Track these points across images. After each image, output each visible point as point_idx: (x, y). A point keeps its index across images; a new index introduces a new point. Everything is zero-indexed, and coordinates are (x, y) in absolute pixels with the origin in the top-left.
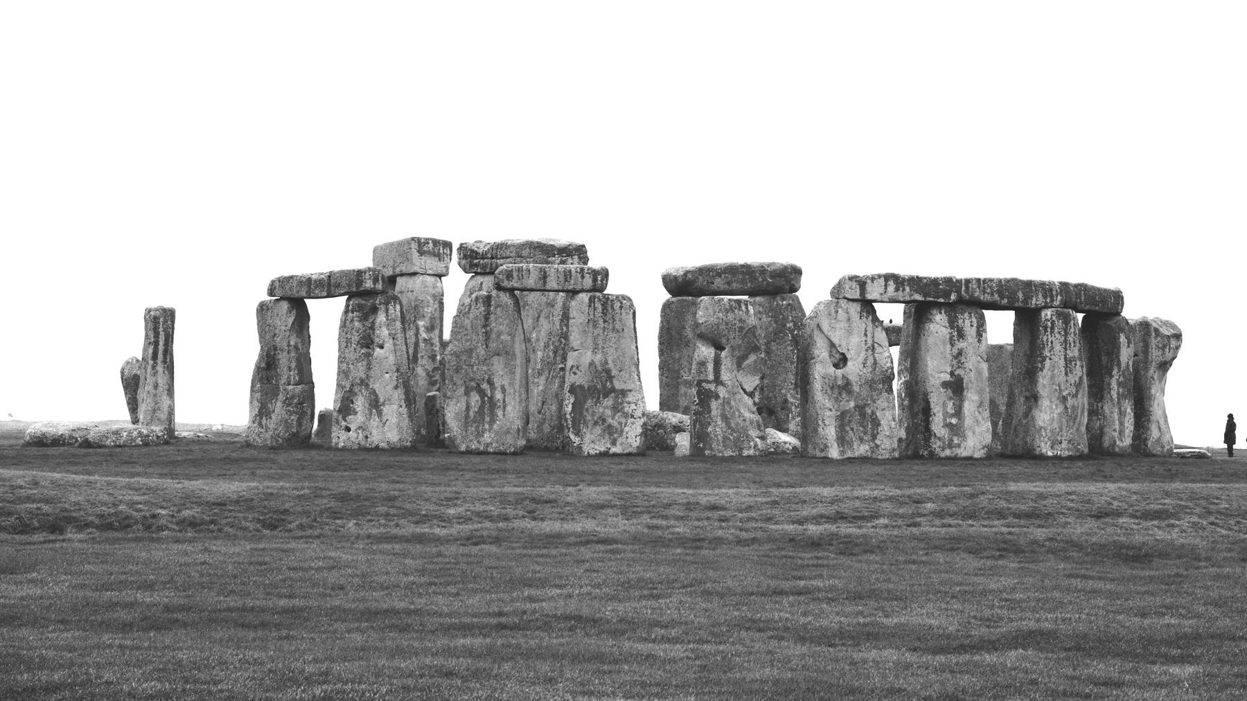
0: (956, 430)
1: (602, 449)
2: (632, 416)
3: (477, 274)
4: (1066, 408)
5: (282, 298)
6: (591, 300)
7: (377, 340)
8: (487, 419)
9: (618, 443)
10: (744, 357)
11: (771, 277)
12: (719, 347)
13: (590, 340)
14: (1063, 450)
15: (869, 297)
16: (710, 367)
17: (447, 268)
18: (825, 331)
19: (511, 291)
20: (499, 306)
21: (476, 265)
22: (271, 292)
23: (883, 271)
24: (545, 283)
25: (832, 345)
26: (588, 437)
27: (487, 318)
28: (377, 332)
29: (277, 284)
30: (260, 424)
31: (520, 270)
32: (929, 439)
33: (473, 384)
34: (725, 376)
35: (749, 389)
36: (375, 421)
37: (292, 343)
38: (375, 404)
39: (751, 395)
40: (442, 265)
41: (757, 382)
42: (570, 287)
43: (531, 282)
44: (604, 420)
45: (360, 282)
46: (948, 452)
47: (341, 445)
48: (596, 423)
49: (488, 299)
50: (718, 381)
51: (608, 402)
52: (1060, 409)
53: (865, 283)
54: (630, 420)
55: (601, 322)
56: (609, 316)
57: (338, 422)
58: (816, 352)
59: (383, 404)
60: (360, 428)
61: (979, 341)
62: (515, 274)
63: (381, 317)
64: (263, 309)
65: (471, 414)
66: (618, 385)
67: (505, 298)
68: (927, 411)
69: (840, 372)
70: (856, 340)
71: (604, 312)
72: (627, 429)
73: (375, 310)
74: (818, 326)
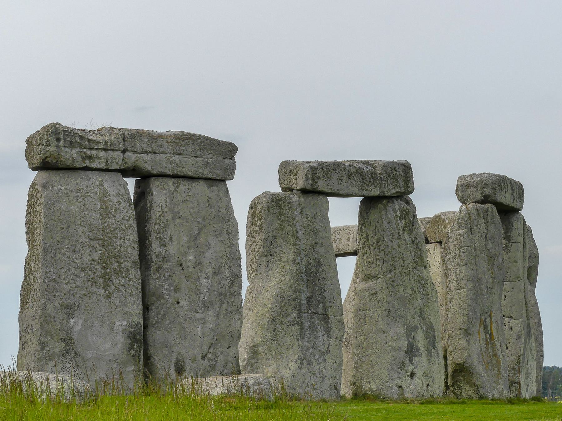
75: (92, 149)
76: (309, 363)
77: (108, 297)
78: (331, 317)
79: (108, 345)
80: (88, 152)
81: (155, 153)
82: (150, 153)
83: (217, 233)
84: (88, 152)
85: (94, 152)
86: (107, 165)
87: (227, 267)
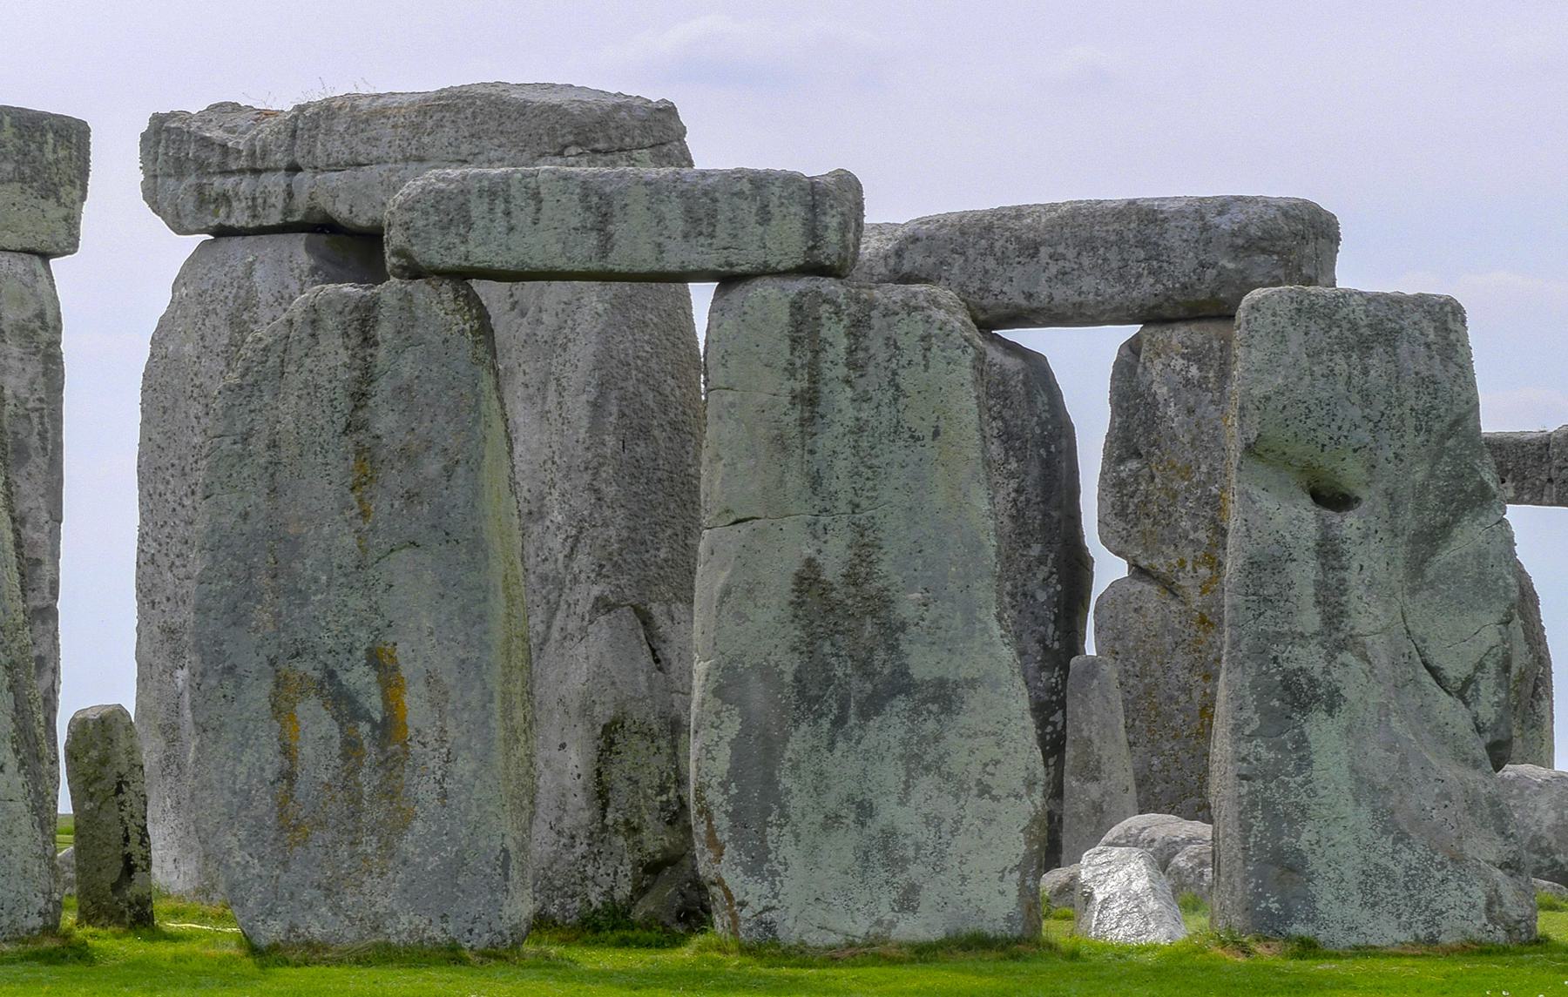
1: (860, 927)
2: (984, 790)
3: (222, 232)
6: (796, 307)
10: (1432, 538)
11: (1236, 251)
13: (795, 481)
16: (1304, 574)
17: (71, 224)
19: (461, 276)
21: (225, 199)
24: (606, 245)
26: (793, 888)
27: (360, 398)
31: (494, 192)
34: (1368, 617)
35: (1455, 670)
39: (1464, 691)
40: (53, 211)
41: (1491, 636)
43: (540, 248)
44: (865, 810)
48: (832, 821)
50: (1335, 630)
51: (889, 730)
54: (974, 806)
55: (844, 396)
62: (478, 209)
65: (301, 787)
66: (923, 664)
72: (961, 842)
75: (232, 173)
80: (218, 183)
81: (360, 165)
82: (347, 164)
83: (531, 390)
84: (218, 183)
85: (230, 181)
86: (254, 216)
87: (556, 494)
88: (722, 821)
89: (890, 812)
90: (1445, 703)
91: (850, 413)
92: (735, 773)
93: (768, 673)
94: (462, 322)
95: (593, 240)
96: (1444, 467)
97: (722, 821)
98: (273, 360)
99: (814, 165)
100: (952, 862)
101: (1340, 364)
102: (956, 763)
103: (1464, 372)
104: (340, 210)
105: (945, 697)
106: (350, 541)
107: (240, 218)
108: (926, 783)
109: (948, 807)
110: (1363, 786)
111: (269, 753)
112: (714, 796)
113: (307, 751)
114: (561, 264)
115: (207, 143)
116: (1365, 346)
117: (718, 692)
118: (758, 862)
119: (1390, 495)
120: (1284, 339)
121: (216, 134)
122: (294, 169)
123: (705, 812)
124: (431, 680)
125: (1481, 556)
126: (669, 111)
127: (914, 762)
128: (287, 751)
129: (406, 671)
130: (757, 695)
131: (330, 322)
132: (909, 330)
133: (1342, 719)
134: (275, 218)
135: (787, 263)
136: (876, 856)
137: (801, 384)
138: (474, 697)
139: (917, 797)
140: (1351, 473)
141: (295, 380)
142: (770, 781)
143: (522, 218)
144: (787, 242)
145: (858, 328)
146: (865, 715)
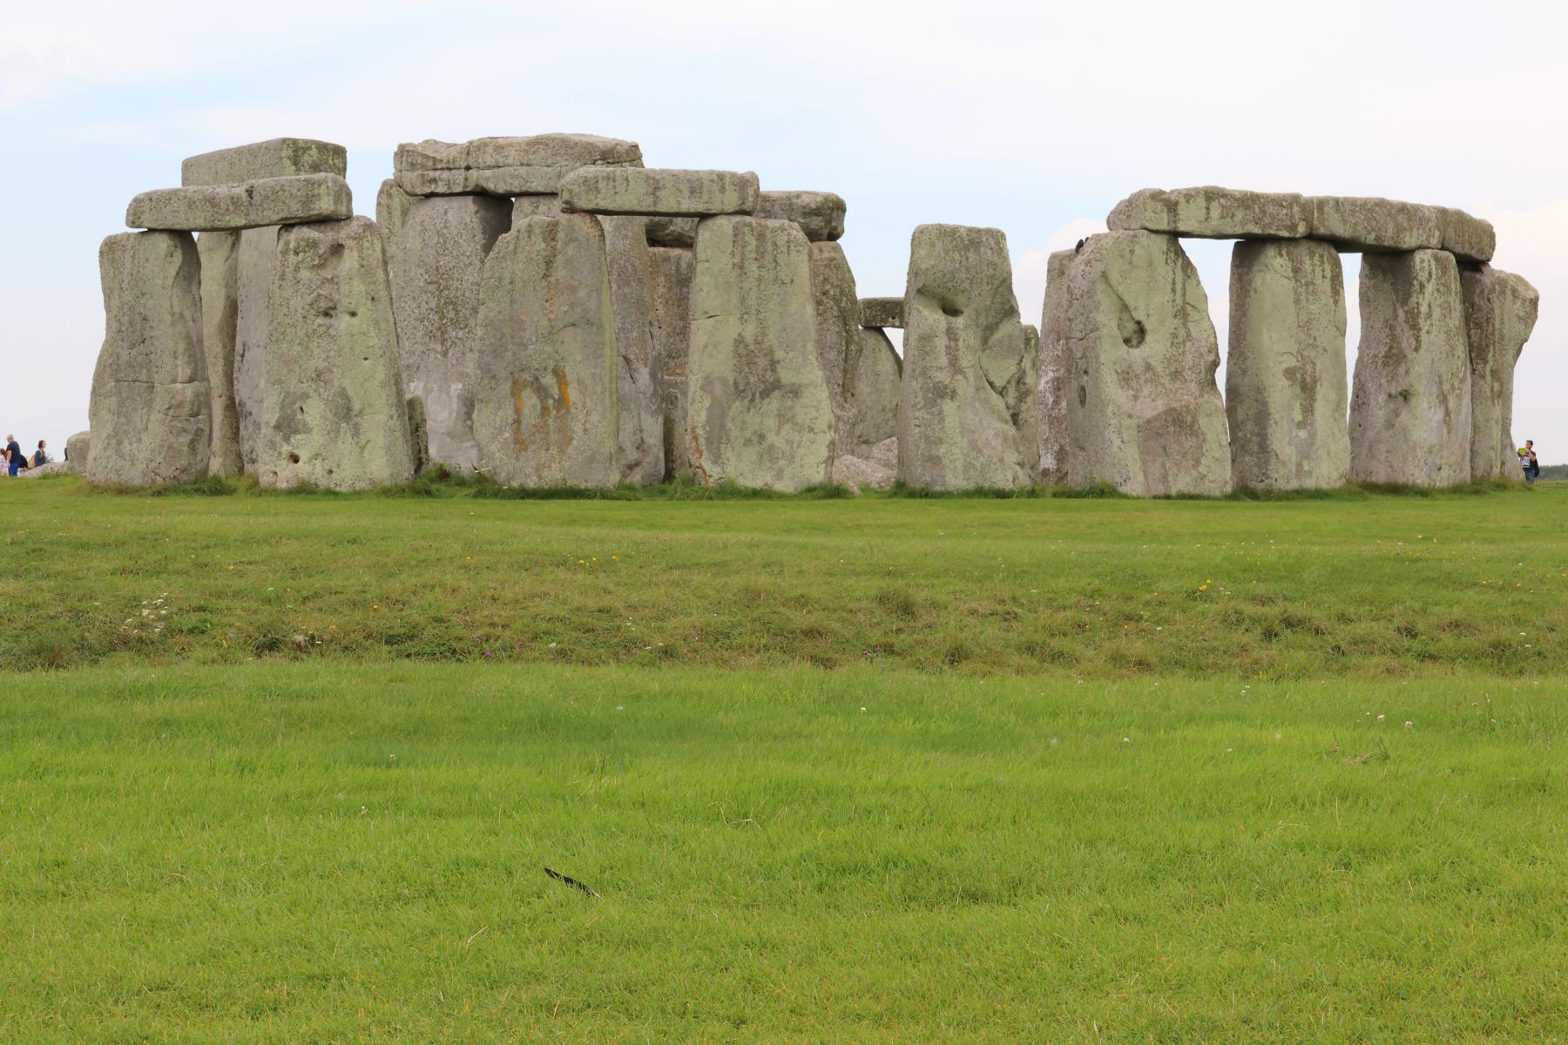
0: (1307, 451)
2: (811, 430)
4: (1447, 413)
5: (151, 231)
6: (735, 228)
7: (344, 303)
8: (554, 437)
9: (787, 473)
10: (990, 329)
12: (951, 310)
14: (1444, 479)
15: (1182, 227)
16: (941, 342)
18: (1114, 282)
19: (593, 213)
20: (571, 240)
21: (434, 180)
22: (132, 223)
23: (1201, 183)
25: (1125, 307)
28: (344, 288)
29: (147, 205)
30: (118, 453)
32: (1267, 462)
33: (526, 376)
34: (966, 361)
35: (999, 383)
36: (346, 444)
37: (177, 309)
38: (345, 412)
39: (1002, 392)
42: (701, 208)
44: (762, 437)
45: (309, 200)
46: (1294, 484)
47: (283, 485)
48: (748, 442)
49: (551, 231)
51: (773, 404)
52: (1439, 415)
53: (1177, 203)
54: (807, 436)
56: (768, 257)
57: (272, 444)
58: (1100, 318)
59: (361, 413)
60: (316, 456)
61: (1336, 302)
62: (601, 185)
63: (350, 260)
64: (111, 250)
65: (523, 427)
66: (786, 376)
67: (582, 224)
68: (1262, 416)
69: (1135, 352)
70: (1162, 298)
71: (761, 254)
72: (802, 451)
73: (337, 249)
74: (1104, 275)
76: (120, 443)
77: (445, 354)
78: (158, 387)
79: (445, 415)
80: (432, 174)
84: (432, 174)
88: (702, 441)
89: (772, 438)
90: (994, 396)
91: (756, 272)
92: (708, 422)
93: (723, 381)
94: (594, 232)
95: (651, 199)
96: (998, 299)
97: (702, 441)
98: (511, 247)
99: (741, 169)
100: (797, 459)
101: (957, 256)
102: (799, 419)
103: (1005, 259)
104: (491, 186)
105: (795, 391)
106: (545, 323)
107: (441, 189)
108: (787, 427)
109: (796, 437)
110: (964, 430)
111: (510, 412)
112: (699, 431)
113: (526, 411)
114: (638, 208)
115: (427, 157)
116: (966, 248)
117: (702, 388)
118: (717, 459)
119: (976, 310)
120: (933, 245)
121: (430, 153)
122: (468, 168)
123: (695, 438)
124: (580, 382)
125: (1010, 336)
126: (636, 147)
127: (784, 418)
128: (517, 411)
129: (569, 378)
130: (718, 389)
131: (537, 231)
132: (782, 239)
133: (956, 403)
134: (459, 189)
135: (732, 210)
136: (766, 457)
137: (737, 260)
138: (599, 389)
139: (783, 432)
140: (960, 301)
141: (521, 256)
142: (722, 425)
143: (621, 189)
144: (731, 201)
145: (761, 237)
146: (762, 398)
